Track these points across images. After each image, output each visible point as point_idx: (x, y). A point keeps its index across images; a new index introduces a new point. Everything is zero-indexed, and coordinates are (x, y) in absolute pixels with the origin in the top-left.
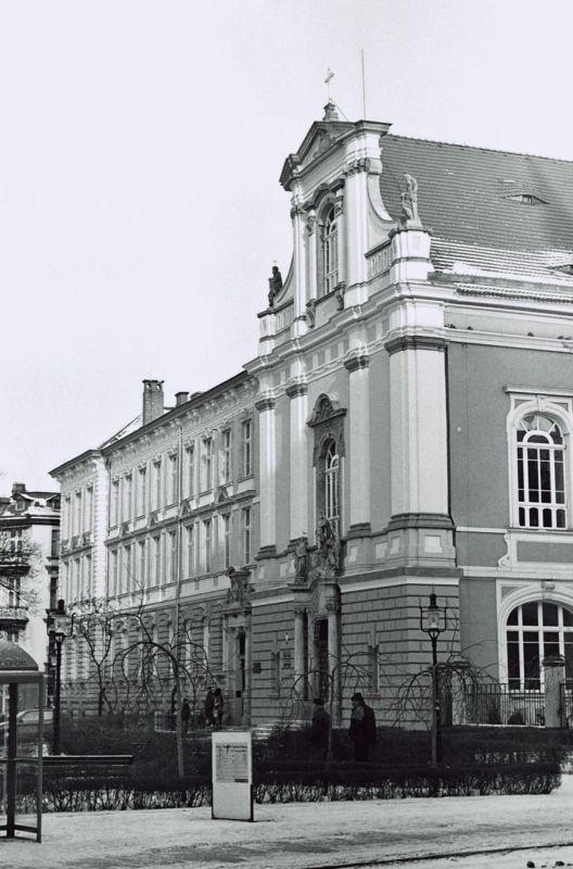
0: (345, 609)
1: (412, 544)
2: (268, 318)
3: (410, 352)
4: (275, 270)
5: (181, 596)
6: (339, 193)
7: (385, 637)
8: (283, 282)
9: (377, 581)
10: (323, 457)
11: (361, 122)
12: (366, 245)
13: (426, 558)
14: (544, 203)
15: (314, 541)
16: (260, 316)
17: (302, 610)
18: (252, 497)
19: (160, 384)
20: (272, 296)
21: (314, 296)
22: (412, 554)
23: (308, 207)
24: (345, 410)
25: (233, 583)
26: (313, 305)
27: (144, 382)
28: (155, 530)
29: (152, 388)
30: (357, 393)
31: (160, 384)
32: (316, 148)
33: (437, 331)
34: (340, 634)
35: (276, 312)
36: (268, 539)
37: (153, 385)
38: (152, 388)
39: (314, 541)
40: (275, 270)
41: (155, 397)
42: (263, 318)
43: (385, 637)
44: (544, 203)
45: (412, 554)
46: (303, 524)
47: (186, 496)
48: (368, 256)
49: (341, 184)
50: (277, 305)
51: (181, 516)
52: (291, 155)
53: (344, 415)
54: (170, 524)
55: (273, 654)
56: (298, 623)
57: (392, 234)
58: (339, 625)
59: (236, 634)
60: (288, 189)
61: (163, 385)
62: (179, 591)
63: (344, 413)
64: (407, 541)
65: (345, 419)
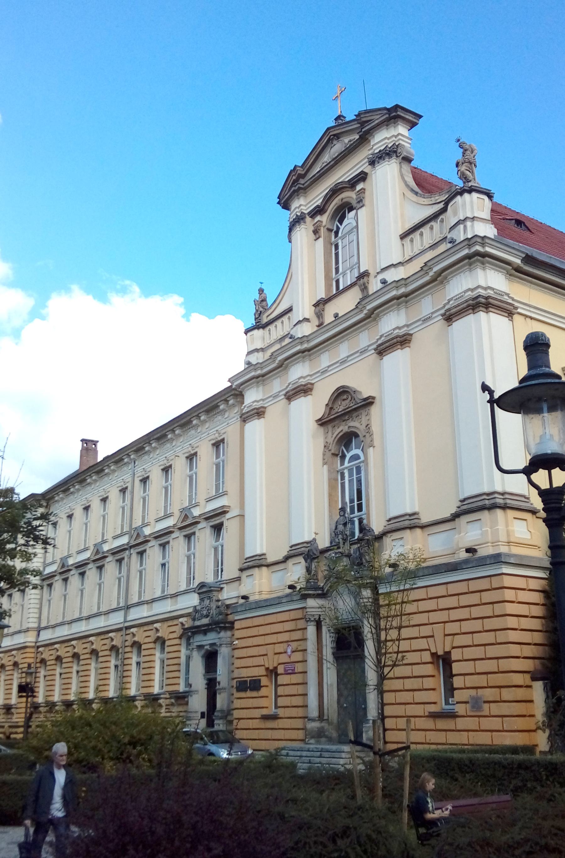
1: (501, 527)
2: (256, 332)
3: (482, 315)
4: (261, 291)
5: (129, 618)
7: (460, 640)
8: (270, 302)
9: (474, 570)
11: (397, 107)
12: (400, 224)
13: (519, 544)
14: (531, 232)
15: (324, 542)
17: (317, 617)
18: (225, 512)
19: (95, 443)
20: (258, 315)
21: (322, 294)
22: (503, 537)
23: (319, 211)
24: (374, 398)
25: (202, 600)
26: (320, 304)
27: (82, 440)
28: (99, 560)
29: (89, 446)
31: (95, 443)
33: (506, 297)
35: (264, 326)
37: (89, 444)
38: (89, 446)
39: (324, 542)
40: (261, 291)
41: (91, 453)
42: (249, 334)
43: (460, 640)
44: (531, 232)
45: (503, 537)
46: (313, 524)
47: (138, 522)
48: (403, 237)
49: (362, 177)
50: (265, 320)
51: (133, 543)
52: (295, 167)
53: (372, 403)
54: (118, 553)
55: (267, 669)
56: (311, 630)
59: (203, 652)
61: (98, 444)
62: (125, 616)
63: (369, 402)
64: (494, 523)
65: (374, 410)
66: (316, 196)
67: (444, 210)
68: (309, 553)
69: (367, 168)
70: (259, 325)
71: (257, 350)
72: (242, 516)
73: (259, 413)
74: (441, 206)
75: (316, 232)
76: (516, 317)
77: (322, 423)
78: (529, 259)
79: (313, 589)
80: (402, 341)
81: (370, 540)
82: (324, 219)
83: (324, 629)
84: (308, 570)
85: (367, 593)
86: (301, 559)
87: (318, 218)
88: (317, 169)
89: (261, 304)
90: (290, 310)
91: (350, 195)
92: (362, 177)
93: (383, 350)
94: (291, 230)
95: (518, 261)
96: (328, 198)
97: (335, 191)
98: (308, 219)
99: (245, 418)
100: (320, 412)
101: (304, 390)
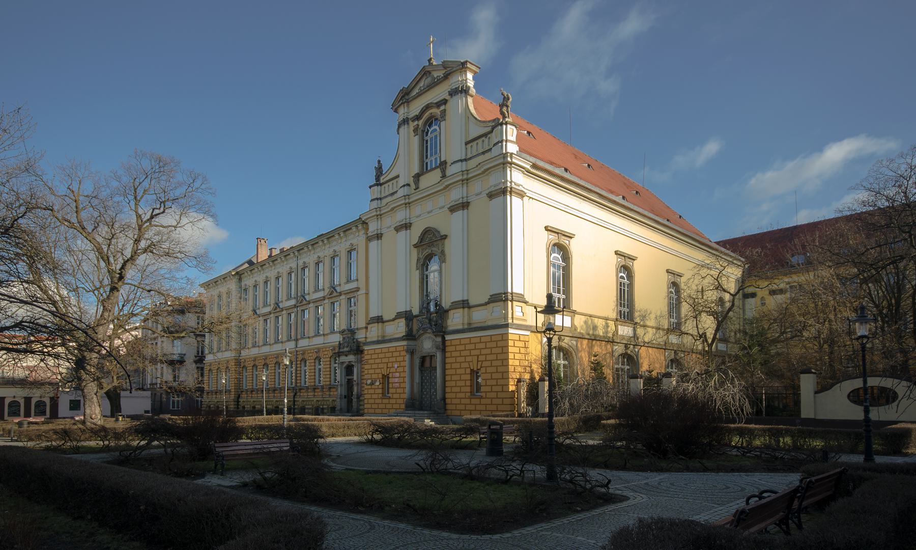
0: (448, 349)
4: (379, 161)
6: (442, 108)
10: (423, 265)
11: (466, 62)
15: (416, 311)
16: (370, 187)
23: (418, 118)
26: (417, 177)
30: (454, 226)
32: (421, 84)
34: (444, 363)
35: (381, 185)
36: (373, 313)
39: (416, 311)
40: (379, 161)
49: (445, 102)
56: (407, 357)
57: (493, 128)
58: (444, 358)
60: (396, 111)
65: (446, 241)
66: (415, 108)
67: (491, 132)
68: (408, 316)
69: (448, 97)
70: (378, 184)
71: (377, 199)
72: (367, 294)
73: (379, 236)
74: (489, 129)
75: (416, 130)
76: (525, 198)
77: (416, 246)
78: (534, 166)
79: (410, 336)
80: (465, 205)
81: (442, 313)
82: (421, 122)
83: (415, 357)
84: (407, 325)
85: (439, 339)
86: (403, 320)
87: (416, 123)
88: (416, 91)
89: (379, 171)
90: (398, 177)
91: (436, 111)
92: (445, 102)
93: (453, 209)
94: (399, 127)
95: (528, 167)
96: (423, 112)
97: (428, 107)
98: (410, 122)
99: (369, 239)
100: (415, 240)
101: (407, 226)
